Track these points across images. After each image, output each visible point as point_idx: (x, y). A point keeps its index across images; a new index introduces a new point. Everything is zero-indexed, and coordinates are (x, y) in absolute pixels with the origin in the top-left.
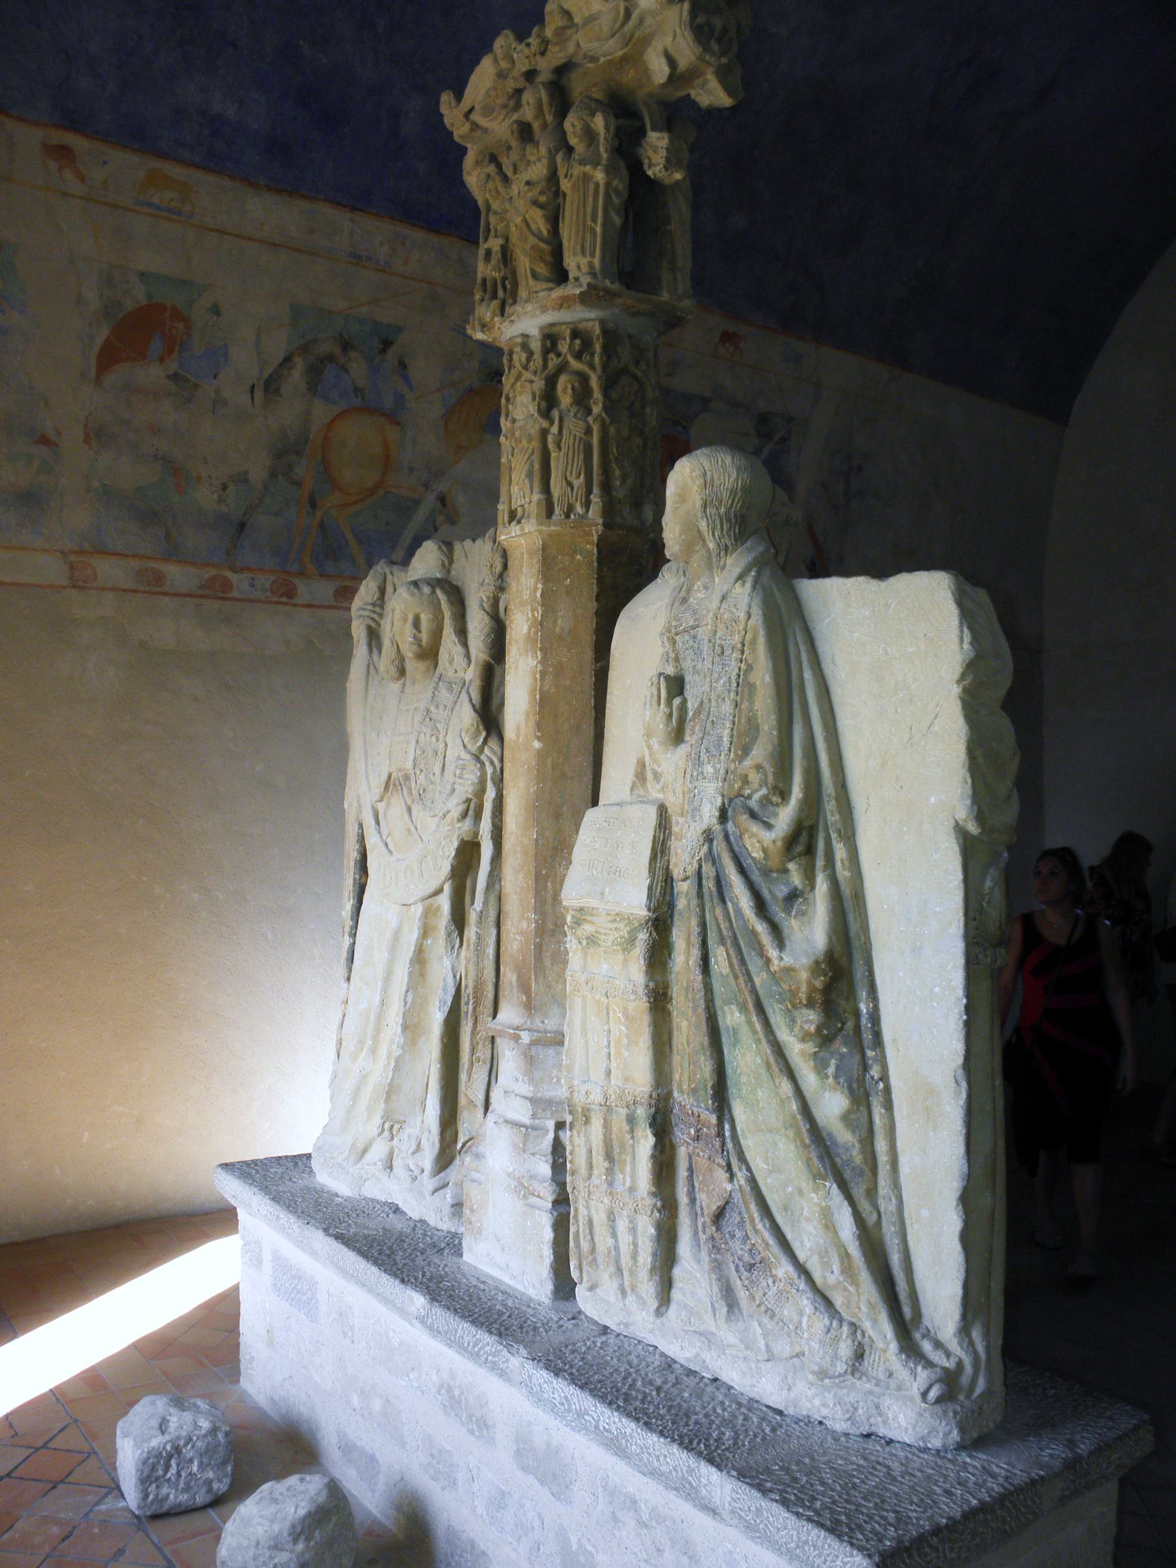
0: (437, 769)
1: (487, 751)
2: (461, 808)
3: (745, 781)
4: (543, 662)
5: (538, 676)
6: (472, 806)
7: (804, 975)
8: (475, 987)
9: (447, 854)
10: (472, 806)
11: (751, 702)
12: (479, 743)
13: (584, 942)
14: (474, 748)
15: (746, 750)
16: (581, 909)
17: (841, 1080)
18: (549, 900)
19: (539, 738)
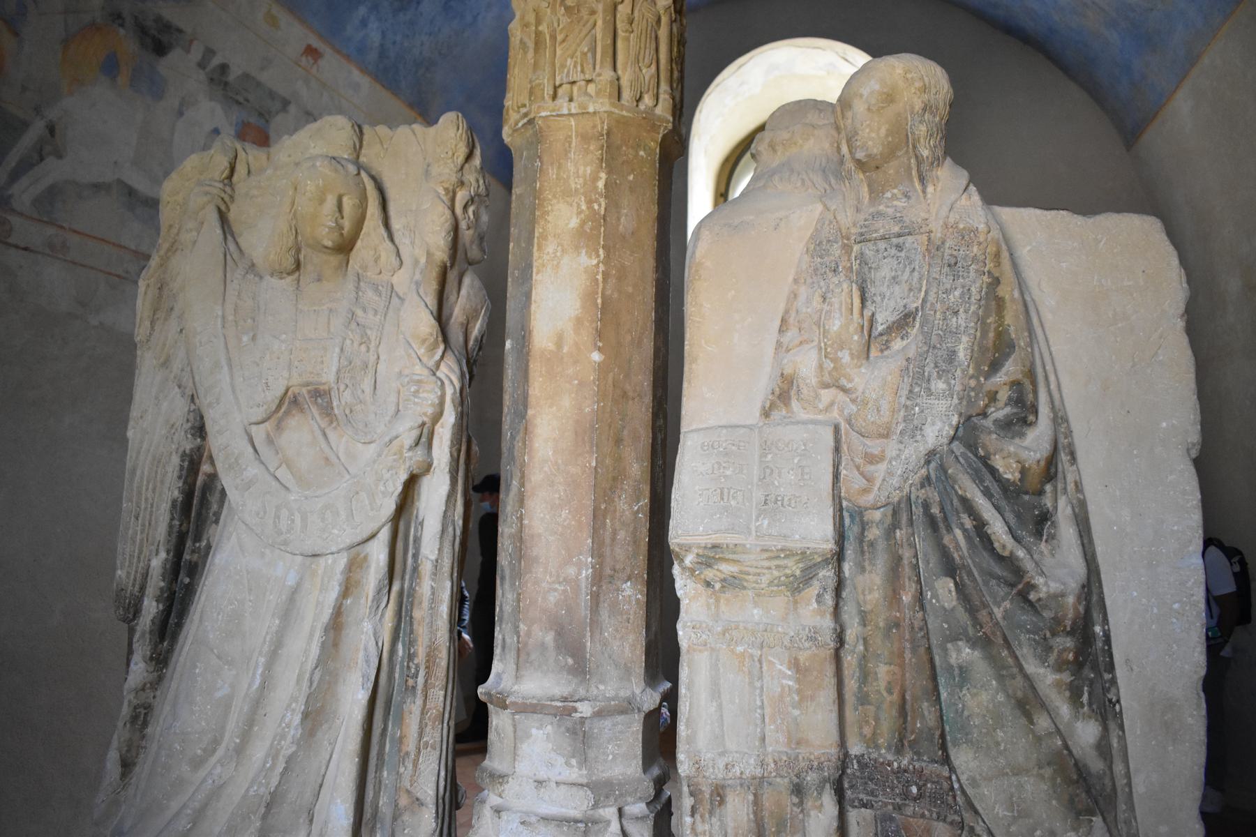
0: (367, 385)
1: (443, 367)
2: (415, 433)
3: (993, 397)
4: (607, 261)
5: (600, 277)
6: (425, 431)
7: (1071, 600)
8: (428, 655)
9: (391, 490)
10: (425, 431)
11: (1000, 316)
12: (437, 357)
13: (718, 586)
14: (431, 363)
15: (995, 366)
16: (714, 547)
17: (1094, 707)
18: (608, 541)
19: (599, 349)
